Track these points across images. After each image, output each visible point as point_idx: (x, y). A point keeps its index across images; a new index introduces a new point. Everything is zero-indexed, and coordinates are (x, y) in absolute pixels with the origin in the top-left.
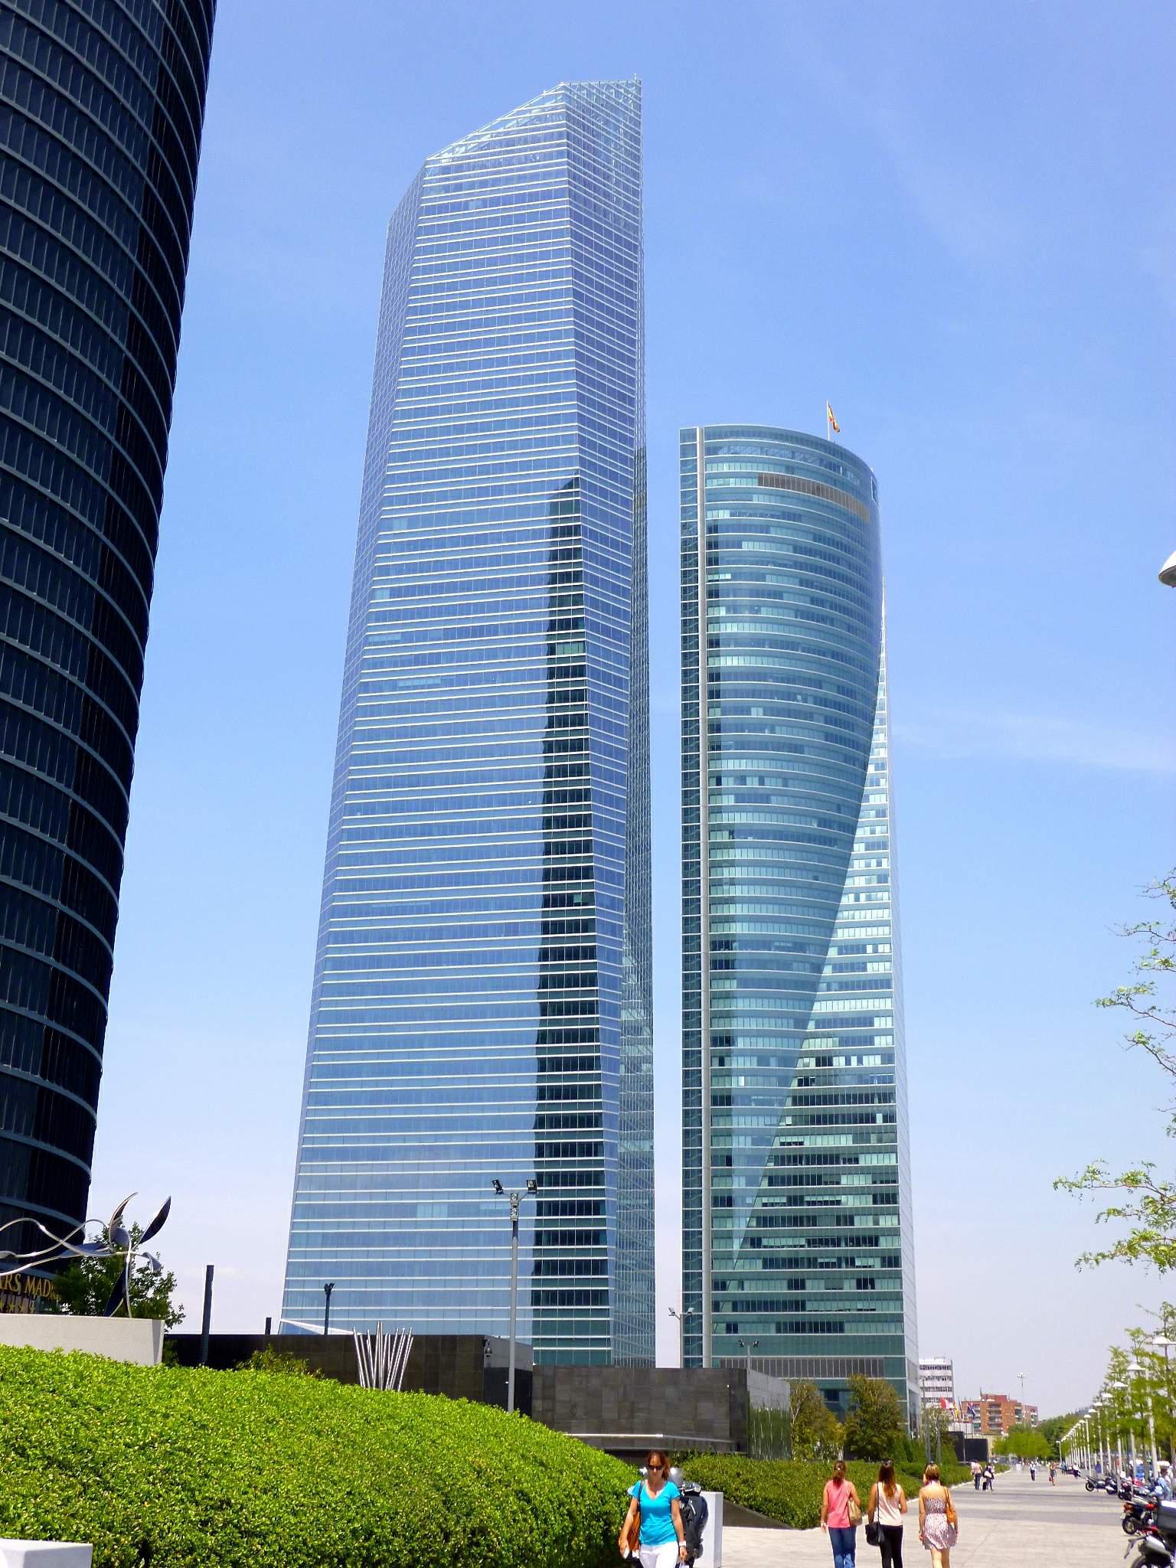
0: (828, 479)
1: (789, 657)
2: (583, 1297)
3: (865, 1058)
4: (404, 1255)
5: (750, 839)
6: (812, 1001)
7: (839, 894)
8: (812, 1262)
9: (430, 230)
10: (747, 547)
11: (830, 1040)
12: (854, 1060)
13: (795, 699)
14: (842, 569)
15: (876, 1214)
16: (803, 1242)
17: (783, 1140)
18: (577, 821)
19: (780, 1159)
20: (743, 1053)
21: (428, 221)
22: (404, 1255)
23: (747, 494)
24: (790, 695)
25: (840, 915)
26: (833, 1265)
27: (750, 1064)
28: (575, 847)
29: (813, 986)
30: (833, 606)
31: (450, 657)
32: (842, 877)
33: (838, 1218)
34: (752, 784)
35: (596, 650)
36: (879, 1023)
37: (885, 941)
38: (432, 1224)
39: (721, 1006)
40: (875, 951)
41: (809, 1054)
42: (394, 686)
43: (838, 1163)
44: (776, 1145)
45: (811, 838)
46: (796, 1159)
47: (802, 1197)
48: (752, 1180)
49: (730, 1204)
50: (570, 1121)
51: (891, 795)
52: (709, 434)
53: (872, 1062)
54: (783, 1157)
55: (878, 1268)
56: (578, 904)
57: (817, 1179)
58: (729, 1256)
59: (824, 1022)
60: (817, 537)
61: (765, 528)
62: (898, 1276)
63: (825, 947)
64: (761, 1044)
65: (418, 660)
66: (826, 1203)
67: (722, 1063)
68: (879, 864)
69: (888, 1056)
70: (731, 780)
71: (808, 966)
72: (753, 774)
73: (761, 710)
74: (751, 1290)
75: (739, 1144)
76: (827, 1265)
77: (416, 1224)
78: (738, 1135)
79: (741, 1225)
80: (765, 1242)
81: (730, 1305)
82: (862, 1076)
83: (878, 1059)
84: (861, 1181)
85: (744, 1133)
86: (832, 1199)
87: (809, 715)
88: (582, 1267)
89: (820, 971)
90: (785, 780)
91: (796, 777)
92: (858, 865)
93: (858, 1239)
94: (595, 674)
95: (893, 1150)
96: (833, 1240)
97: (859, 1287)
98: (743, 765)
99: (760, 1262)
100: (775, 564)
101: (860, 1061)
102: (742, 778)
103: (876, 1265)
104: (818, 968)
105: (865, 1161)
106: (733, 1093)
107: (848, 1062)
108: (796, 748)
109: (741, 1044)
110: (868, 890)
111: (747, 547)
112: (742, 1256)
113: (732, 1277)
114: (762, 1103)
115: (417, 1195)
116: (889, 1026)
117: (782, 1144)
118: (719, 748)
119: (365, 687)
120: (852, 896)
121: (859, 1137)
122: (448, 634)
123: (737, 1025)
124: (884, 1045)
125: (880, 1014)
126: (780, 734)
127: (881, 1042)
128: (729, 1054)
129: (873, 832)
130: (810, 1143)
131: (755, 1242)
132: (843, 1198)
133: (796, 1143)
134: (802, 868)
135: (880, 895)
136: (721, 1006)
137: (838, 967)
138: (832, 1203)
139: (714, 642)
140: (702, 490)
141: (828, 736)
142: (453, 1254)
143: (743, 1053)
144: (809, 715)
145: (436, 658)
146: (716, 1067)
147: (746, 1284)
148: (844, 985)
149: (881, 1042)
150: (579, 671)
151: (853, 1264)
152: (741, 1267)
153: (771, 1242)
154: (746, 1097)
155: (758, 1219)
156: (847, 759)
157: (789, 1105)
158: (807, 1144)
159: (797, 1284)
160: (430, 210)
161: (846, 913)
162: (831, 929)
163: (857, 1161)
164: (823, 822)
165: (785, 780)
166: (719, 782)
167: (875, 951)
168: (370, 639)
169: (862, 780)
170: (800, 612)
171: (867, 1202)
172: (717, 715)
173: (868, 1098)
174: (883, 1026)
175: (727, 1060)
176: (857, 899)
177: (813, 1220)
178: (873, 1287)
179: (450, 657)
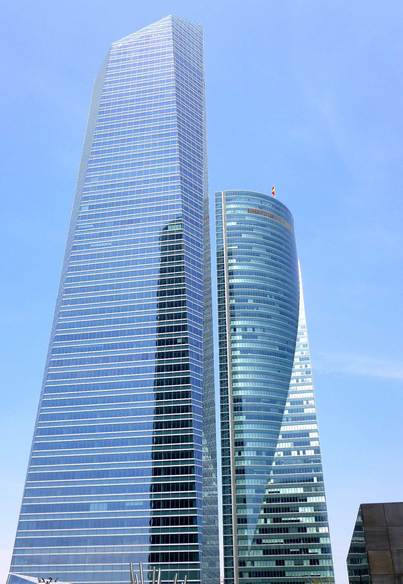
0: (276, 213)
1: (263, 279)
2: (184, 557)
3: (306, 451)
4: (82, 533)
5: (249, 354)
6: (280, 426)
7: (289, 379)
8: (287, 551)
9: (112, 68)
10: (243, 236)
11: (289, 444)
12: (301, 452)
13: (267, 297)
14: (283, 247)
15: (317, 526)
16: (282, 541)
17: (270, 490)
18: (179, 304)
19: (270, 500)
20: (249, 449)
21: (110, 65)
22: (82, 533)
23: (244, 215)
24: (265, 295)
25: (290, 388)
26: (298, 553)
27: (253, 454)
28: (178, 316)
29: (280, 419)
30: (281, 261)
31: (116, 233)
32: (290, 372)
33: (299, 529)
34: (250, 331)
35: (187, 228)
36: (312, 435)
37: (312, 399)
38: (98, 515)
39: (238, 428)
40: (308, 403)
41: (280, 450)
42: (88, 246)
43: (297, 501)
44: (267, 493)
45: (276, 354)
46: (277, 500)
47: (281, 519)
48: (256, 510)
49: (246, 522)
50: (176, 455)
51: (309, 338)
52: (226, 194)
53: (310, 453)
54: (270, 499)
55: (320, 553)
56: (180, 343)
57: (287, 509)
58: (246, 549)
59: (287, 435)
60: (272, 234)
61: (252, 229)
62: (330, 558)
63: (284, 403)
64: (257, 445)
65: (101, 235)
66: (292, 521)
67: (240, 454)
68: (306, 366)
69: (317, 450)
70: (240, 329)
71: (277, 410)
72: (250, 326)
73: (252, 301)
74: (257, 565)
75: (249, 493)
76: (295, 553)
77: (89, 515)
78: (248, 488)
79: (250, 532)
80: (263, 541)
81: (247, 574)
82: (306, 460)
83: (313, 451)
84: (309, 510)
85: (251, 487)
86: (295, 519)
87: (273, 303)
88: (183, 538)
89: (283, 413)
90: (264, 329)
91: (269, 329)
92: (296, 367)
93: (309, 539)
94: (187, 238)
95: (323, 495)
96: (297, 540)
97: (311, 564)
98: (245, 323)
99: (261, 552)
100: (255, 243)
101: (304, 453)
102: (245, 328)
103: (319, 552)
104: (282, 411)
105: (310, 500)
106: (245, 469)
107: (299, 453)
108: (269, 316)
109: (248, 445)
110: (302, 377)
111: (243, 236)
112: (253, 549)
113: (249, 559)
114: (259, 473)
115: (91, 498)
116: (317, 437)
117: (270, 492)
118: (234, 316)
119: (75, 248)
120: (295, 380)
121: (306, 488)
122: (115, 223)
123: (245, 436)
124: (315, 445)
126: (261, 310)
127: (313, 444)
128: (243, 450)
129: (302, 353)
131: (259, 541)
132: (301, 519)
133: (276, 492)
134: (274, 367)
135: (307, 379)
136: (238, 428)
137: (291, 411)
138: (295, 521)
139: (231, 273)
140: (224, 215)
142: (110, 532)
143: (249, 449)
144: (273, 303)
145: (110, 234)
146: (237, 456)
147: (255, 563)
148: (294, 419)
149: (313, 444)
150: (180, 236)
151: (308, 552)
152: (253, 554)
153: (267, 541)
154: (252, 471)
155: (260, 530)
156: (289, 322)
157: (272, 474)
158: (281, 493)
159: (280, 562)
160: (112, 62)
161: (293, 388)
162: (286, 394)
163: (306, 500)
164: (281, 348)
165: (264, 329)
166: (235, 330)
167: (308, 403)
168: (79, 227)
169: (296, 332)
170: (266, 262)
171: (312, 520)
172: (233, 302)
173: (309, 470)
174: (314, 437)
175: (242, 452)
176: (297, 381)
177: (286, 530)
178: (318, 564)
179: (116, 233)
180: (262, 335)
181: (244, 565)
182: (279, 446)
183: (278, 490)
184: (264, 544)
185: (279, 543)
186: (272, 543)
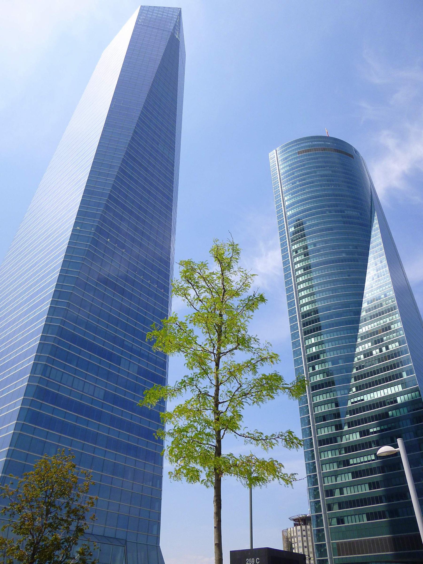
6: (357, 330)
12: (384, 349)
17: (352, 400)
19: (353, 412)
29: (358, 321)
41: (360, 353)
47: (368, 430)
74: (348, 493)
80: (351, 462)
101: (387, 348)
107: (381, 351)
113: (336, 486)
117: (352, 403)
125: (392, 323)
130: (367, 398)
141: (345, 223)
146: (311, 371)
147: (345, 489)
157: (353, 381)
164: (347, 253)
173: (394, 366)
180: (323, 248)
181: (332, 495)
182: (359, 349)
183: (362, 398)
184: (352, 465)
185: (369, 461)
186: (362, 463)
